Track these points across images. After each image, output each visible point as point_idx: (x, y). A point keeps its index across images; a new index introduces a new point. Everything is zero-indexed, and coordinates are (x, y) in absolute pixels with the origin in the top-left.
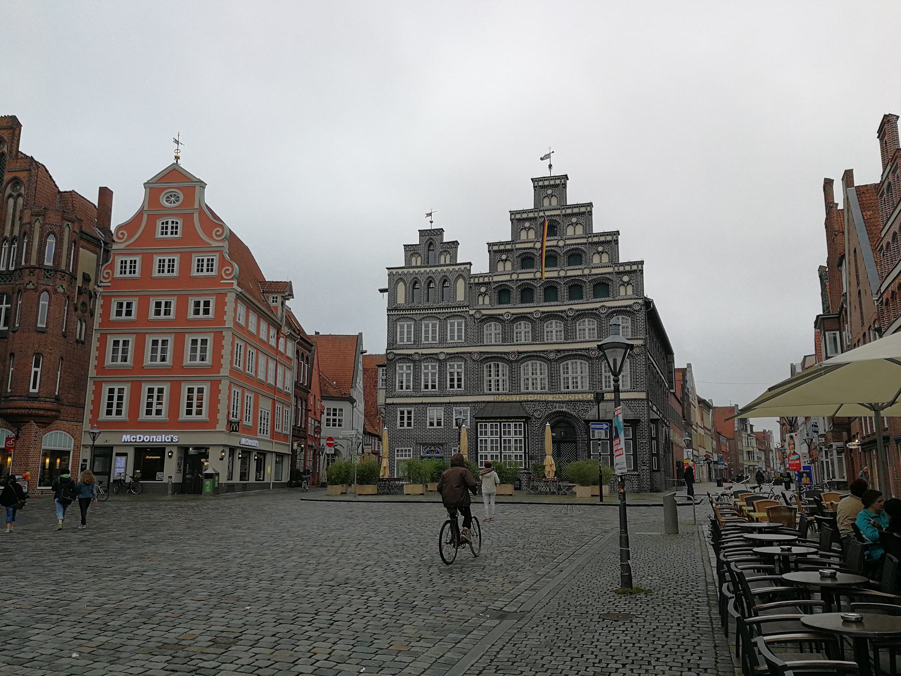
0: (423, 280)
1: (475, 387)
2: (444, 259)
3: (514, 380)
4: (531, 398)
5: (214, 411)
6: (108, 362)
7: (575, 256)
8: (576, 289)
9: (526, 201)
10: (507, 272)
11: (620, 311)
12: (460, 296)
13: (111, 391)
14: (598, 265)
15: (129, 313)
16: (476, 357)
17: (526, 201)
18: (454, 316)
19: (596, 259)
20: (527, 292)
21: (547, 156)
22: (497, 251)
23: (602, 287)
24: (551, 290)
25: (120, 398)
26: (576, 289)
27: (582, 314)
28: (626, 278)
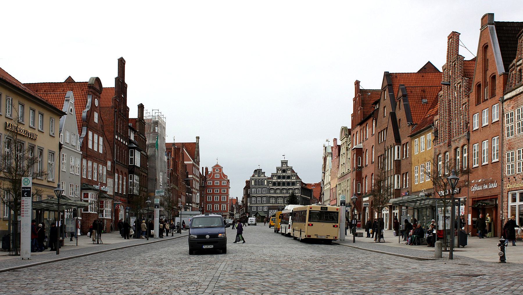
0: (258, 180)
1: (268, 202)
2: (262, 176)
3: (276, 201)
4: (279, 205)
5: (227, 209)
6: (208, 200)
7: (289, 177)
8: (288, 184)
9: (280, 165)
10: (275, 179)
11: (297, 189)
12: (266, 184)
13: (209, 205)
14: (294, 179)
15: (211, 192)
16: (269, 197)
17: (280, 165)
18: (264, 188)
19: (293, 178)
20: (279, 184)
21: (284, 155)
22: (273, 175)
23: (293, 184)
24: (284, 184)
25: (210, 207)
26: (288, 184)
27: (290, 189)
28: (298, 182)
